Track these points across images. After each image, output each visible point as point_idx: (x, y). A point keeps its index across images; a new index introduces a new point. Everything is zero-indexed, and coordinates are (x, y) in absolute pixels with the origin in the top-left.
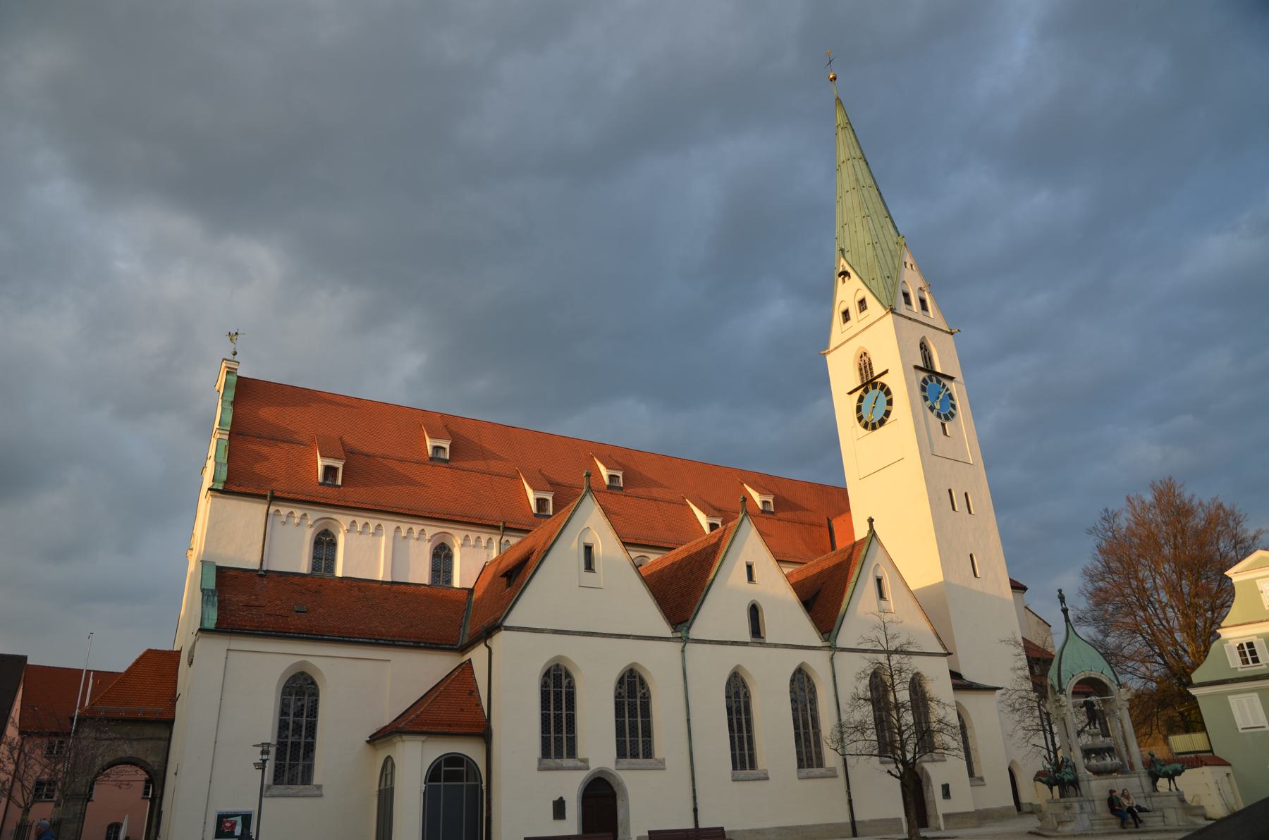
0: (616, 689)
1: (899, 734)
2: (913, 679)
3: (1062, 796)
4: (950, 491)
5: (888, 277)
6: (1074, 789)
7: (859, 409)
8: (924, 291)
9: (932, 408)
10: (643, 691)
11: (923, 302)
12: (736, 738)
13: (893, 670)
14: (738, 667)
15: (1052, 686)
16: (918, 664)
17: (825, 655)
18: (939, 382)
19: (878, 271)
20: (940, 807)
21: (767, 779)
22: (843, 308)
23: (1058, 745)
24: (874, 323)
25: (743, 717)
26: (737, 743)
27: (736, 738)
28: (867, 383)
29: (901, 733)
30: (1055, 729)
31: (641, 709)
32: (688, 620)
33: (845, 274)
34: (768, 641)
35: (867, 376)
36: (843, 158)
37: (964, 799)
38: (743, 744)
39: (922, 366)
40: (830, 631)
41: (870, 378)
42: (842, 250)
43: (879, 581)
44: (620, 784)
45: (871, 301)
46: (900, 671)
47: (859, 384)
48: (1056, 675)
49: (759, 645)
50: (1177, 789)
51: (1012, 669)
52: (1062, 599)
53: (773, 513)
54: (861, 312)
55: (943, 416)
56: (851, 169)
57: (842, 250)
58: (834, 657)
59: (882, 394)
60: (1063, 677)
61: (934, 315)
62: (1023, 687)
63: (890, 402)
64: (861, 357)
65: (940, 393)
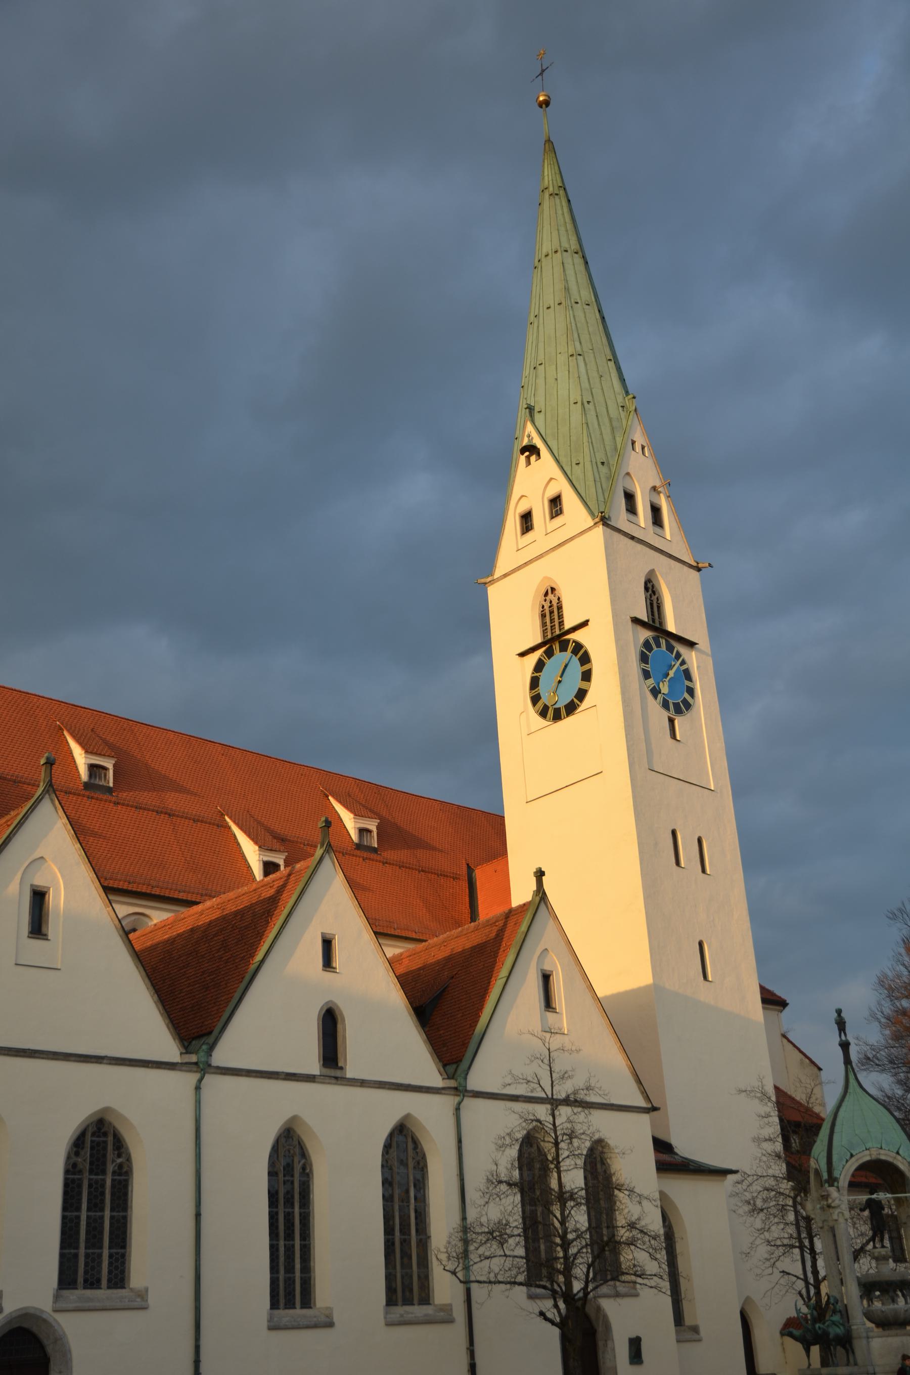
0: (68, 1158)
1: (562, 1246)
2: (591, 1150)
3: (825, 1363)
4: (674, 833)
5: (603, 463)
6: (843, 1351)
7: (535, 683)
8: (659, 493)
9: (655, 692)
10: (119, 1161)
11: (656, 511)
13: (558, 1133)
14: (294, 1119)
15: (817, 1173)
17: (446, 1103)
18: (670, 648)
19: (586, 450)
21: (330, 1325)
22: (523, 508)
23: (822, 1273)
24: (572, 539)
25: (297, 1210)
28: (552, 640)
29: (566, 1245)
30: (818, 1245)
31: (113, 1194)
32: (210, 1033)
33: (531, 450)
34: (349, 1075)
35: (553, 627)
36: (546, 247)
38: (293, 1260)
39: (646, 619)
40: (458, 1061)
41: (558, 632)
42: (530, 409)
43: (546, 978)
44: (60, 1340)
45: (570, 501)
46: (571, 1135)
47: (539, 640)
48: (824, 1154)
49: (334, 1081)
52: (841, 1025)
53: (375, 850)
54: (552, 517)
56: (558, 269)
57: (530, 409)
58: (461, 1106)
59: (575, 660)
61: (671, 535)
62: (771, 1172)
63: (587, 676)
64: (546, 594)
65: (671, 667)
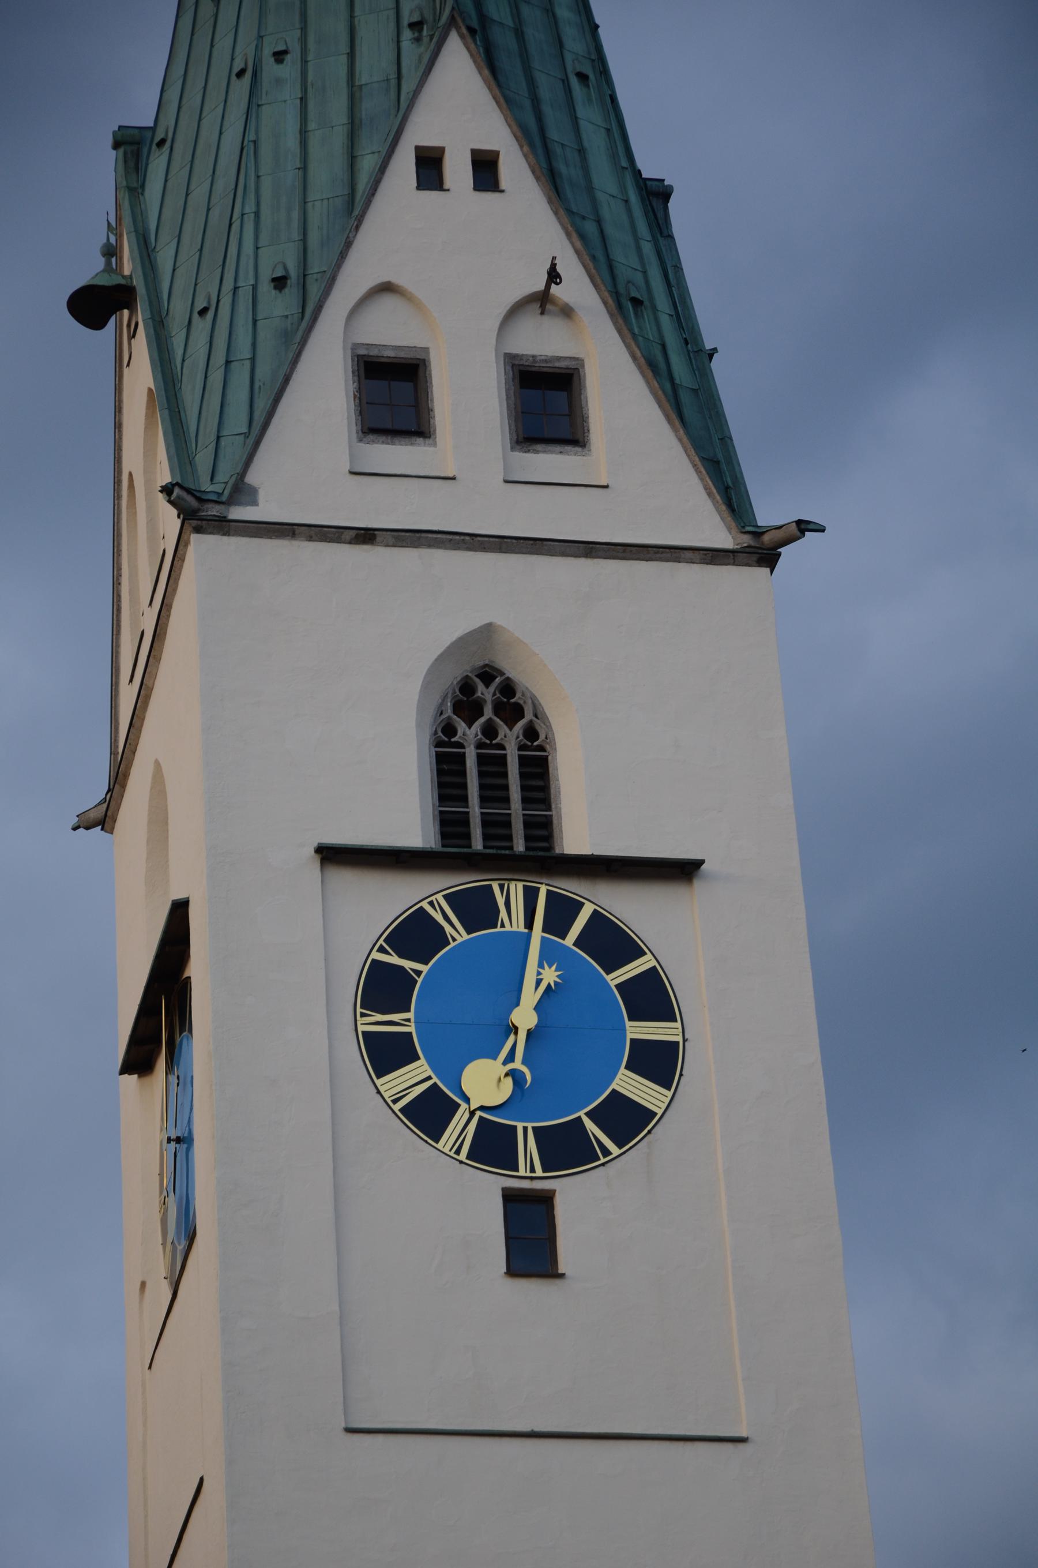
55: (528, 1149)
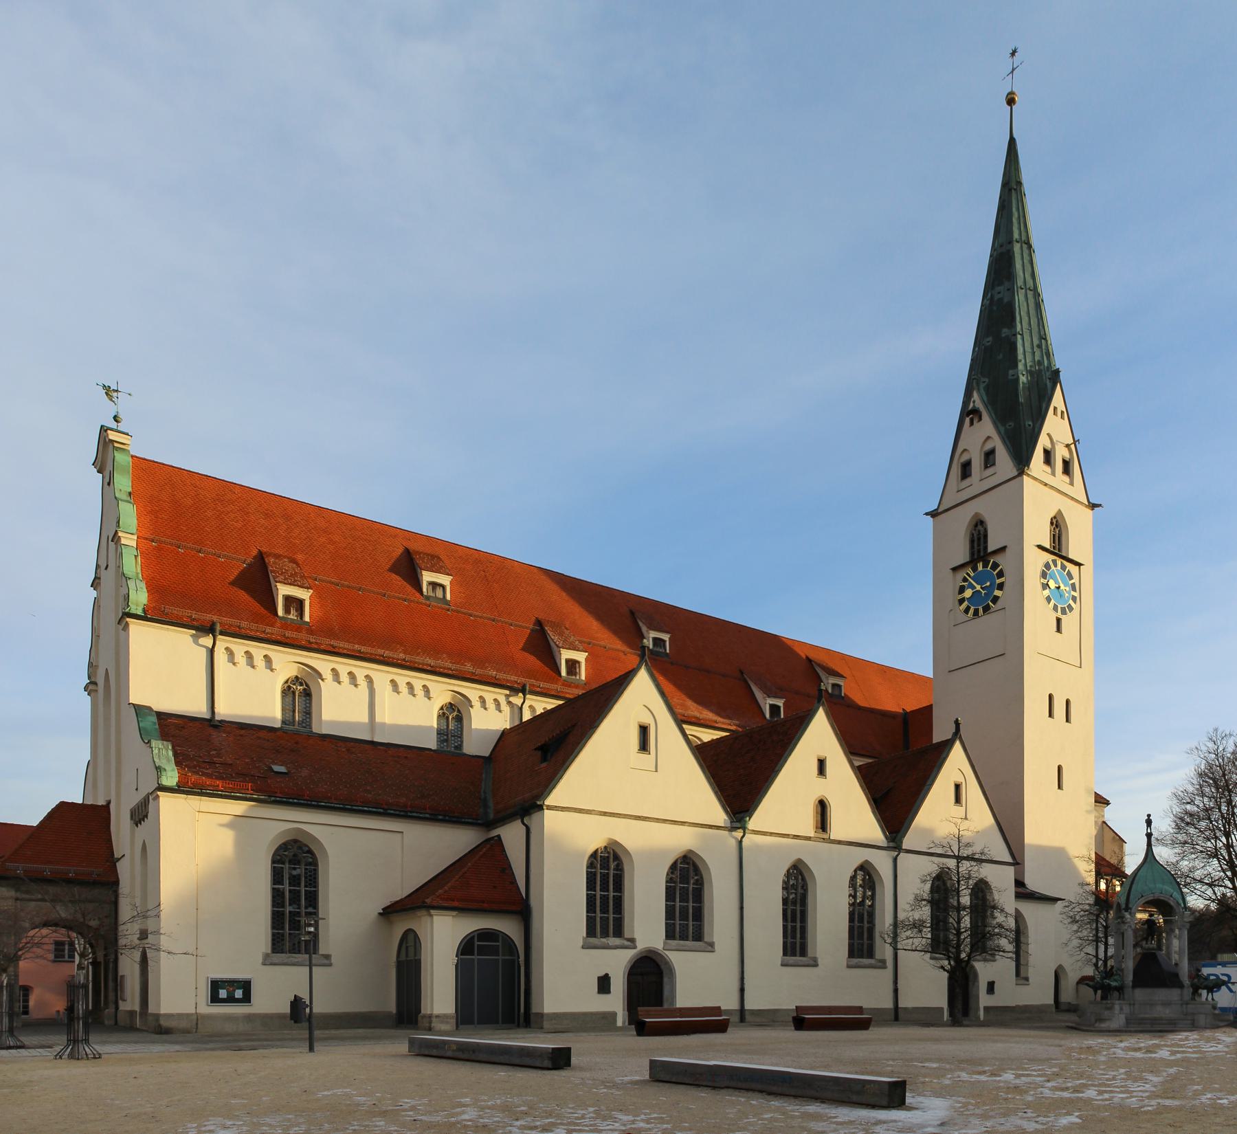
3: (1104, 998)
12: (789, 927)
15: (1119, 904)
16: (987, 872)
20: (984, 1000)
23: (1109, 954)
25: (798, 908)
26: (789, 931)
27: (789, 927)
29: (959, 933)
30: (1111, 941)
37: (1010, 995)
50: (1213, 999)
51: (1079, 884)
52: (1149, 822)
60: (1132, 897)
62: (1088, 902)
